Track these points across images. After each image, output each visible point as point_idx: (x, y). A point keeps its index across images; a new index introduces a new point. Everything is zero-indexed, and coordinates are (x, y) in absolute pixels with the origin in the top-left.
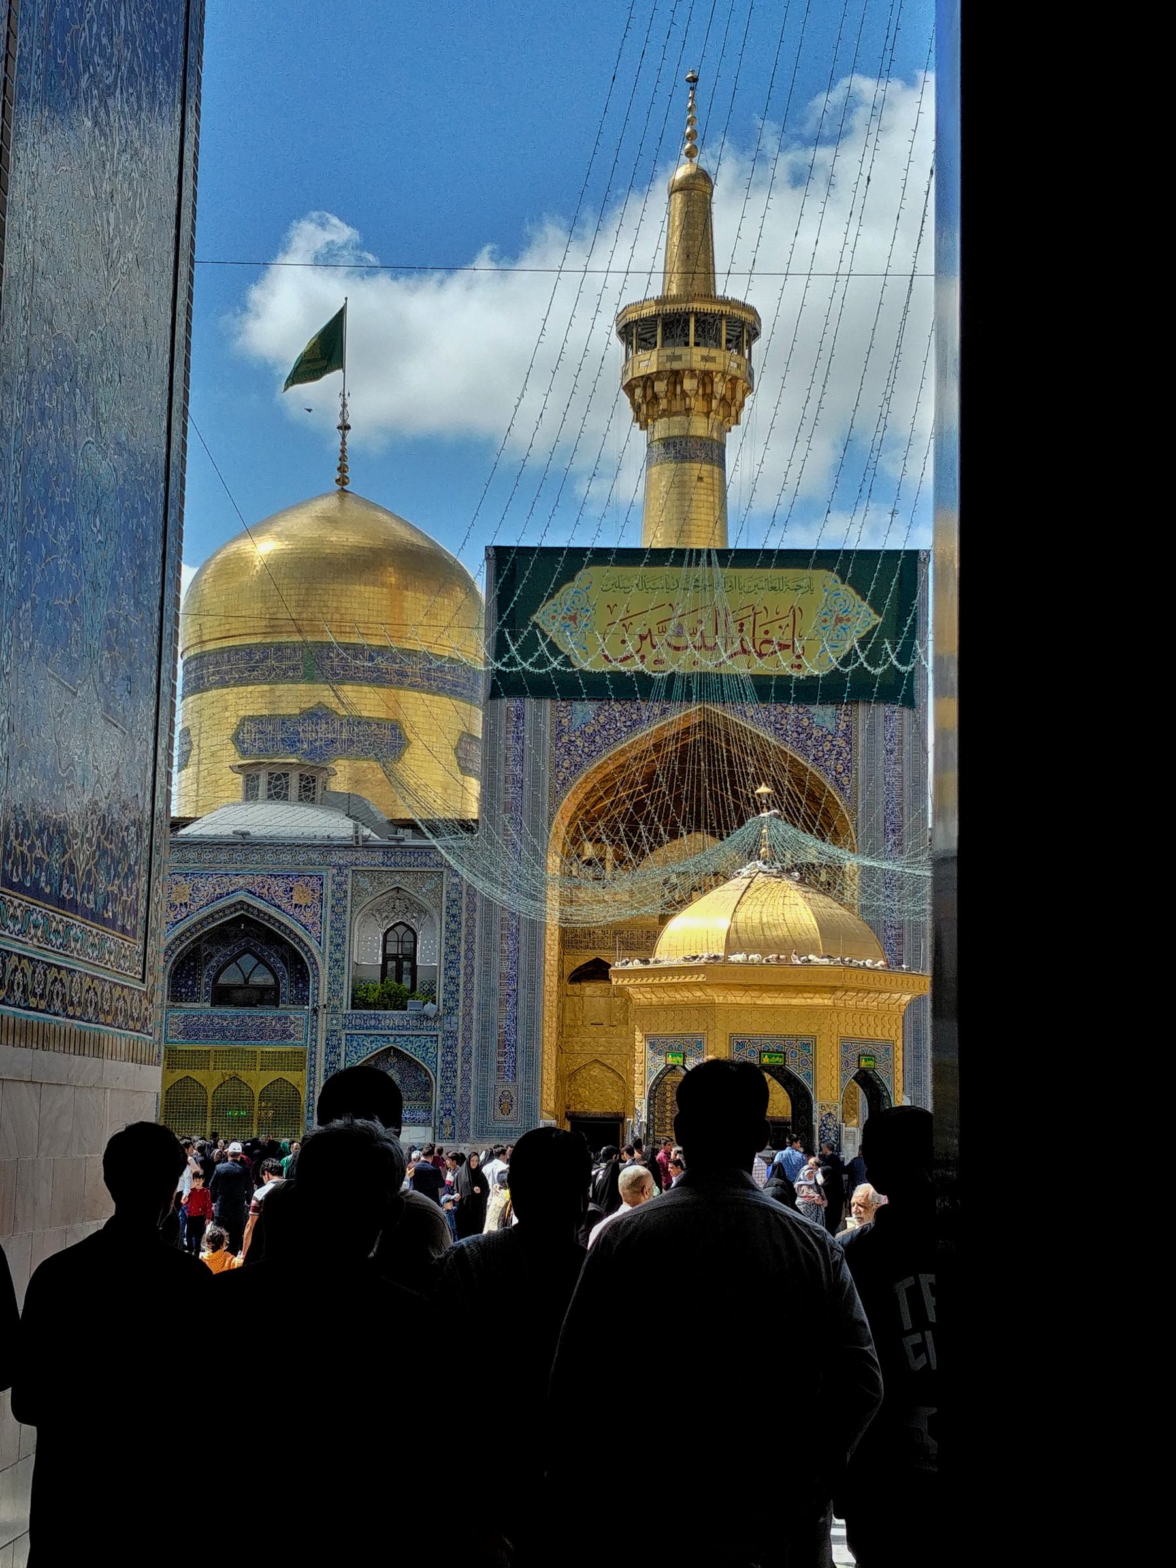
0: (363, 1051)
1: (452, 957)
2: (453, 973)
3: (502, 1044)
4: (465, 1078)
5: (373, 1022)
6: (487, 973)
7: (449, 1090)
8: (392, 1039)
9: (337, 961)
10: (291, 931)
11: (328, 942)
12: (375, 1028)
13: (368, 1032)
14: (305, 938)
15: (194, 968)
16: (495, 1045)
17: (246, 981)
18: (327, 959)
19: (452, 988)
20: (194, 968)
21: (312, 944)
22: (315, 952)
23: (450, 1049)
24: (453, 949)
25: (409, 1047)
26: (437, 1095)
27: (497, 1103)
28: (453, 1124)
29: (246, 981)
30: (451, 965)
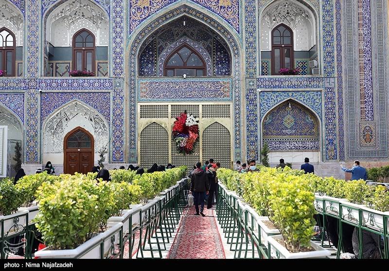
0: (272, 102)
1: (328, 39)
2: (329, 49)
3: (362, 96)
4: (340, 119)
5: (277, 83)
6: (350, 50)
7: (331, 127)
8: (290, 94)
9: (251, 43)
10: (219, 24)
11: (244, 31)
12: (280, 87)
13: (275, 90)
14: (228, 28)
15: (152, 55)
16: (358, 97)
17: (185, 63)
18: (244, 42)
19: (329, 59)
20: (152, 55)
21: (233, 32)
22: (235, 38)
23: (330, 100)
24: (329, 33)
25: (302, 99)
26: (323, 129)
27: (362, 135)
28: (335, 149)
29: (185, 63)
30: (328, 44)
